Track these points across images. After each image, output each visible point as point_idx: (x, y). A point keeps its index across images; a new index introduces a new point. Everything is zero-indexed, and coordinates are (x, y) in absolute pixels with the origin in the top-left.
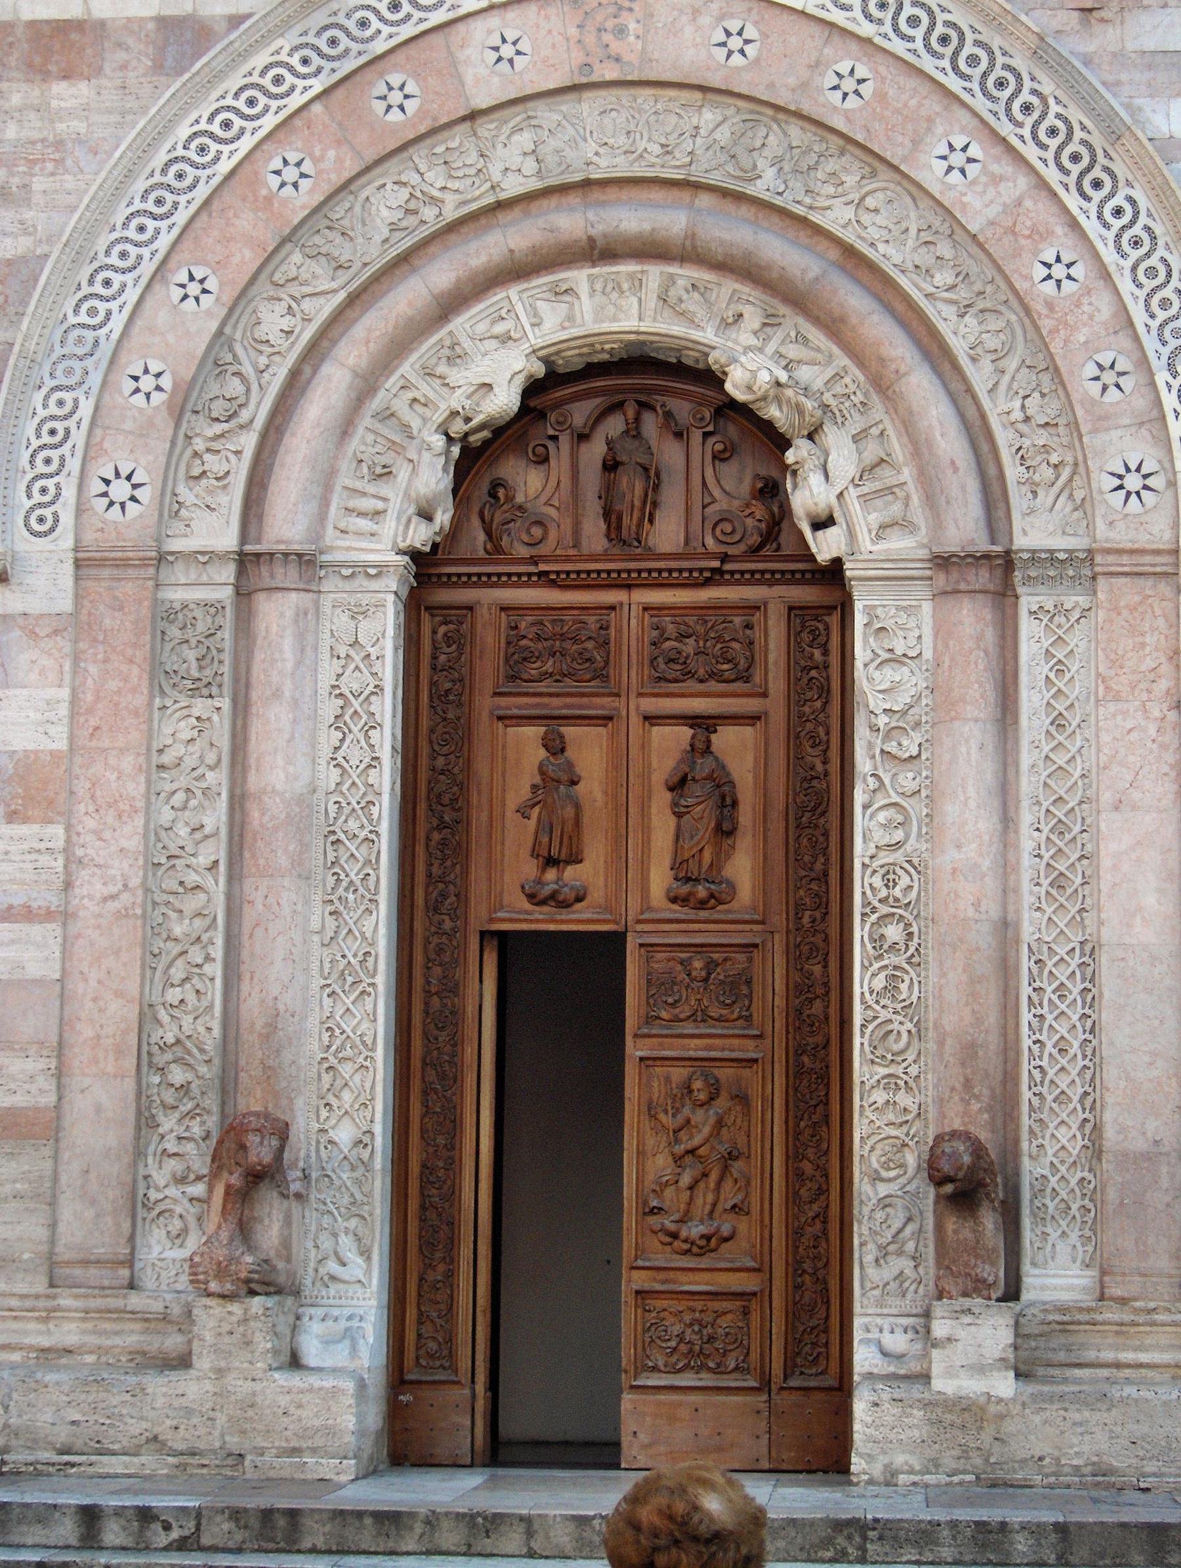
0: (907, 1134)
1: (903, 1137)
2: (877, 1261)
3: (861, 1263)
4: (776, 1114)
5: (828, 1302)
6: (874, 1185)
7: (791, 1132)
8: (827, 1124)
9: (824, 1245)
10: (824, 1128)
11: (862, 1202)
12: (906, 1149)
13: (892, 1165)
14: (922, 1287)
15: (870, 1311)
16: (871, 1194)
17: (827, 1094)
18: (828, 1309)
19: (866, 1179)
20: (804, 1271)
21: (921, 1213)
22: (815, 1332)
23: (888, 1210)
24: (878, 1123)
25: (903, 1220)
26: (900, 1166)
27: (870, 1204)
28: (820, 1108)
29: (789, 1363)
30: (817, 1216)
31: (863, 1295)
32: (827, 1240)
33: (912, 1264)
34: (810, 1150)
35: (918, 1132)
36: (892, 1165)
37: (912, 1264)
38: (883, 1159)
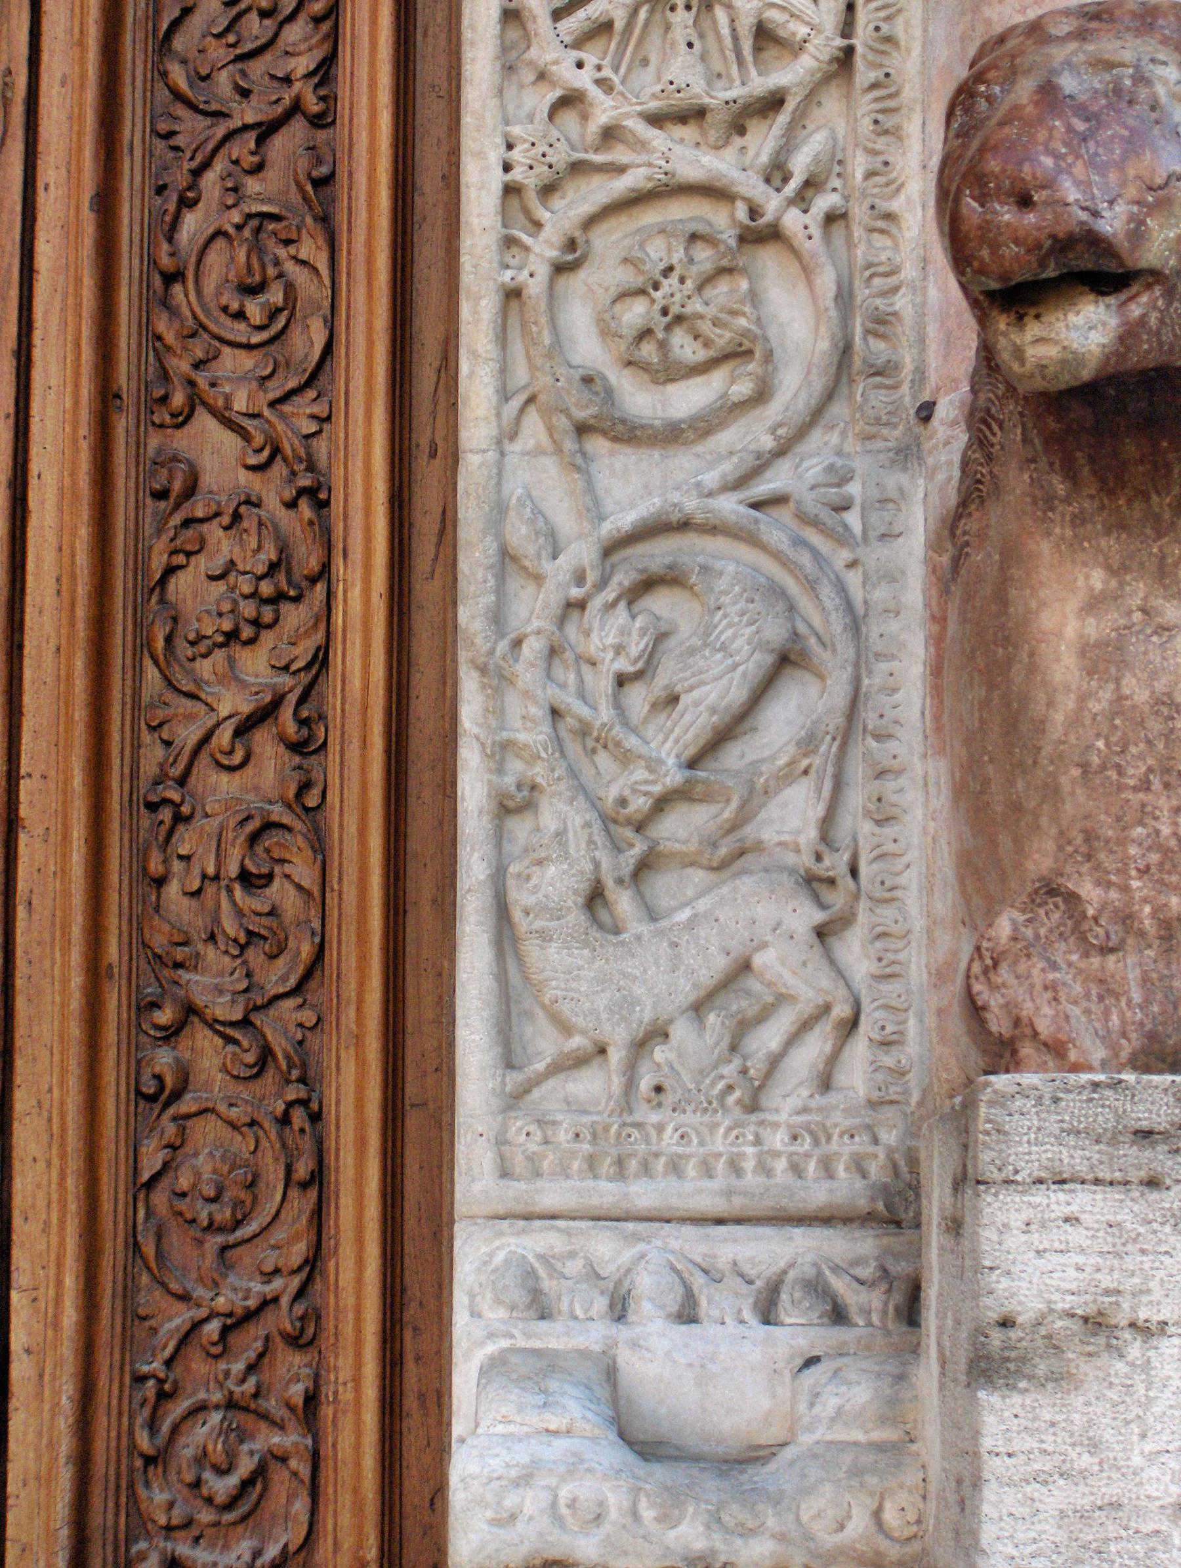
0: (776, 173)
1: (752, 186)
2: (595, 898)
3: (502, 912)
4: (50, 172)
5: (318, 1178)
6: (579, 465)
7: (129, 266)
8: (325, 221)
9: (304, 871)
10: (311, 248)
11: (507, 557)
12: (769, 259)
13: (684, 347)
14: (859, 1048)
15: (552, 1196)
16: (565, 519)
17: (325, 71)
18: (318, 1215)
19: (533, 424)
20: (190, 1011)
21: (856, 626)
22: (249, 1342)
23: (661, 603)
24: (604, 109)
25: (756, 664)
26: (737, 354)
27: (558, 571)
28: (294, 135)
29: (100, 1514)
30: (265, 714)
31: (514, 1100)
32: (319, 846)
33: (807, 915)
34: (231, 362)
35: (836, 161)
36: (684, 347)
37: (807, 915)
38: (636, 313)
